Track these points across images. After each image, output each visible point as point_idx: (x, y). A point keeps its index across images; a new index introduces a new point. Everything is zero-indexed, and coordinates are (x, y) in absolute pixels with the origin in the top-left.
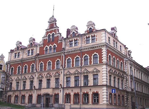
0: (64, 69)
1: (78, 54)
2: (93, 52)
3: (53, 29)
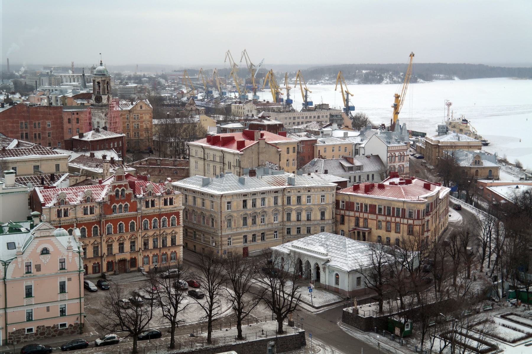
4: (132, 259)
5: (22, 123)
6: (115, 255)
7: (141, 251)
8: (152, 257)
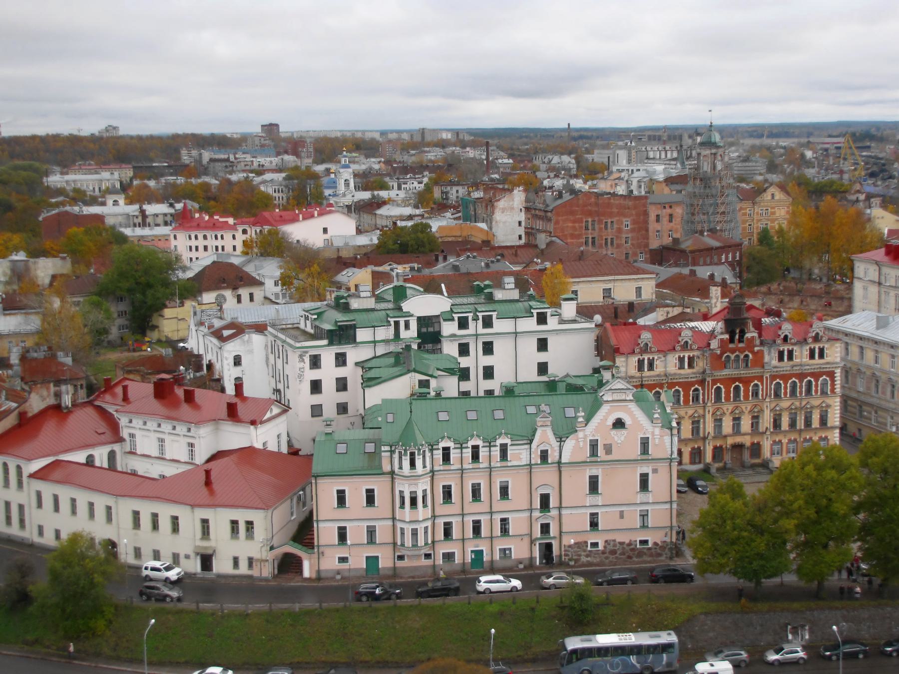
1: (796, 376)
2: (821, 374)
4: (753, 444)
5: (587, 222)
6: (725, 436)
7: (768, 433)
8: (788, 443)
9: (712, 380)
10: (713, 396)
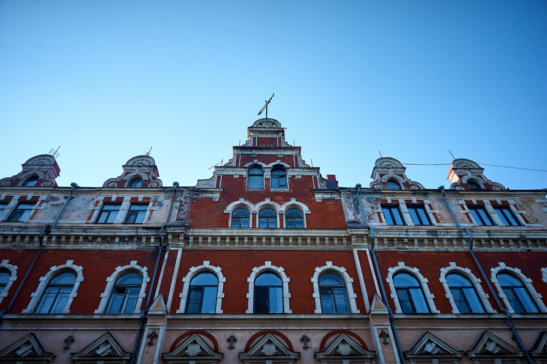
0: (392, 320)
3: (281, 153)
9: (184, 251)
10: (184, 295)
